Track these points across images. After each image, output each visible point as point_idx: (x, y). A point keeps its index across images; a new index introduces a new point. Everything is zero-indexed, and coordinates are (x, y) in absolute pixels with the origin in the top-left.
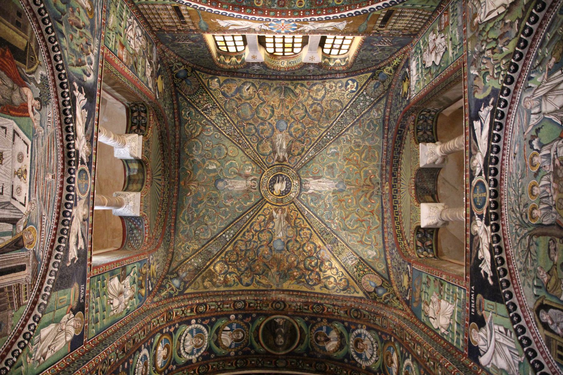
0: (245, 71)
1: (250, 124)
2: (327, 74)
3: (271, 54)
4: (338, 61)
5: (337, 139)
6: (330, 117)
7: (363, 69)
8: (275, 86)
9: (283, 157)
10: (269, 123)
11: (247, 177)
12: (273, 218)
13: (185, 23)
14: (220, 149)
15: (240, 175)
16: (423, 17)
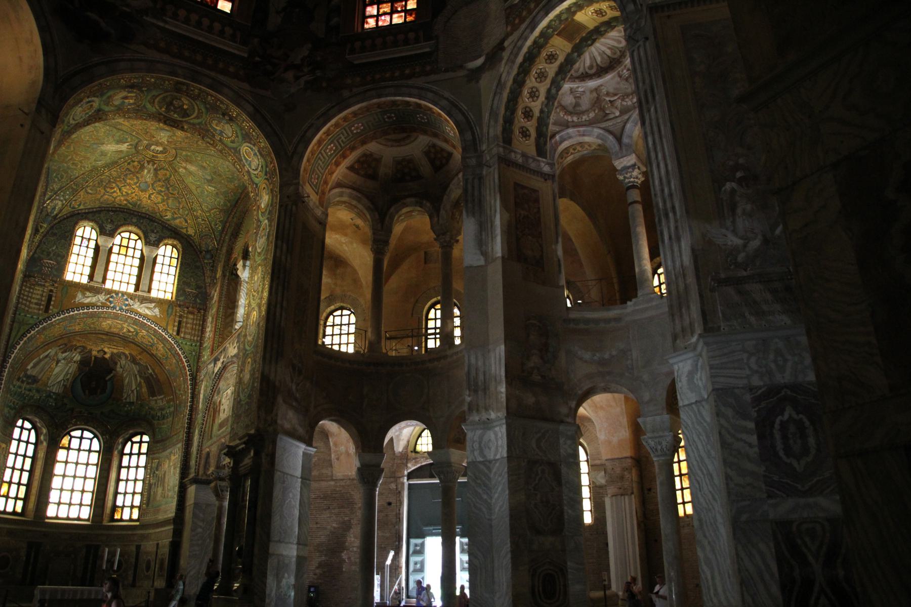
0: (165, 231)
1: (172, 194)
2: (96, 211)
3: (140, 238)
4: (85, 224)
5: (95, 168)
6: (99, 183)
7: (64, 219)
8: (144, 209)
9: (149, 164)
10: (155, 190)
11: (185, 168)
12: (168, 142)
13: (181, 316)
14: (201, 193)
15: (190, 173)
16: (24, 302)
